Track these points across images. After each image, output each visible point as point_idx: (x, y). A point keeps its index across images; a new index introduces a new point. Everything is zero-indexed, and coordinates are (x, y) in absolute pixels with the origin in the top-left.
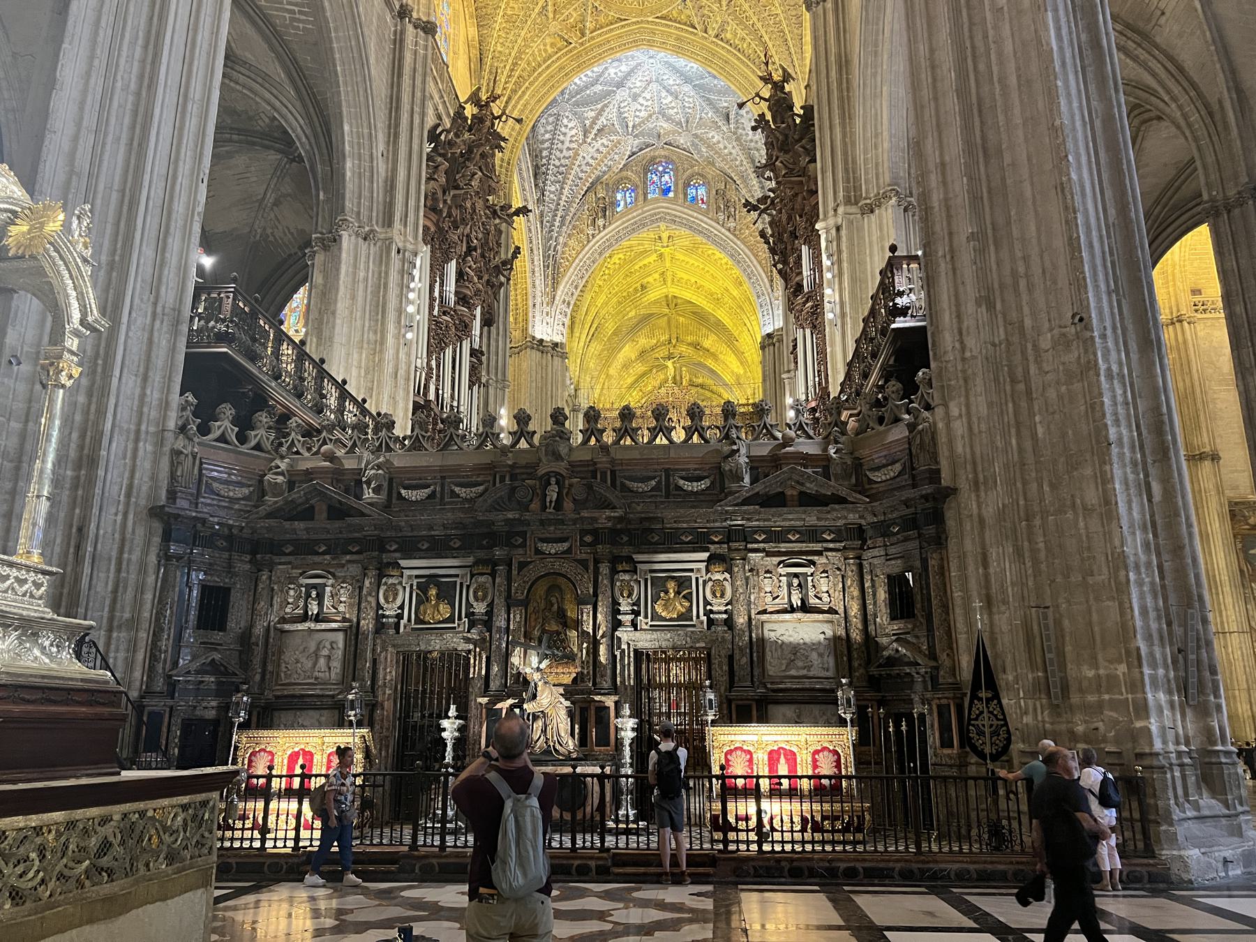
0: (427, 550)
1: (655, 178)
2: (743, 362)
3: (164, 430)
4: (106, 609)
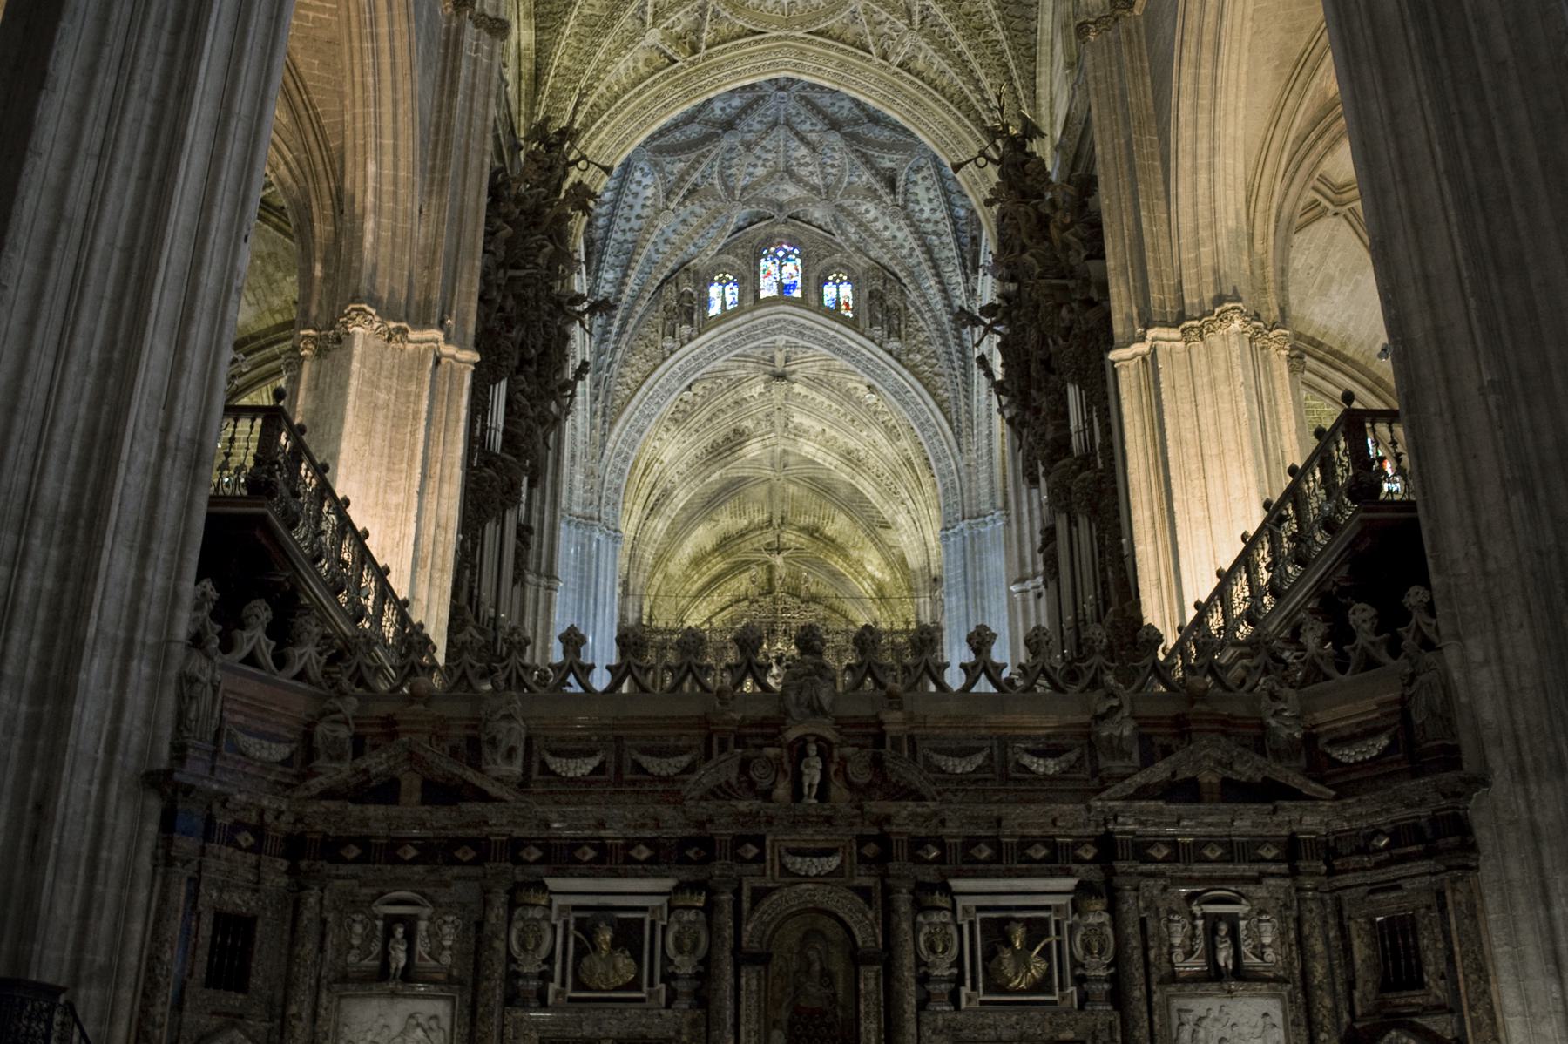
0: (589, 862)
1: (774, 269)
3: (169, 641)
4: (69, 946)
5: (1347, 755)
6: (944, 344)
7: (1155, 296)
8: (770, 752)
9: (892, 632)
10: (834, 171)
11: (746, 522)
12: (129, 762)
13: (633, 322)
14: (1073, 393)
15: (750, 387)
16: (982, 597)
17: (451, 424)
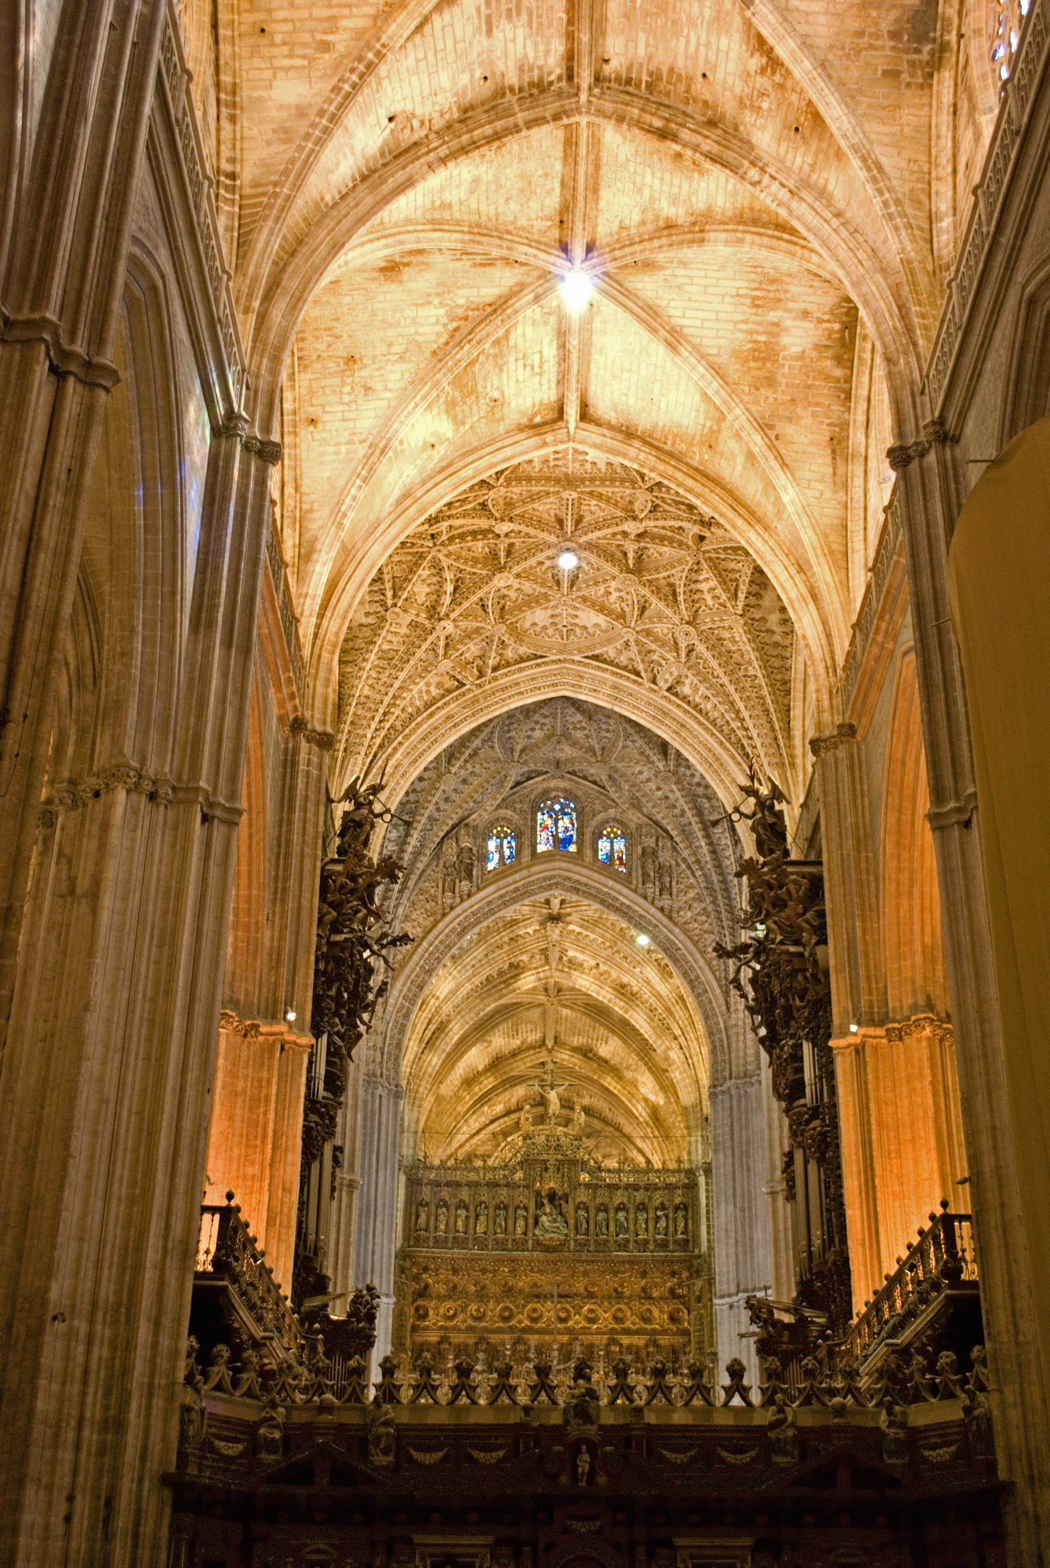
1: (549, 822)
2: (667, 1087)
7: (864, 998)
9: (665, 1170)
10: (609, 735)
11: (518, 1042)
12: (153, 1466)
14: (807, 1050)
15: (526, 927)
16: (748, 1157)
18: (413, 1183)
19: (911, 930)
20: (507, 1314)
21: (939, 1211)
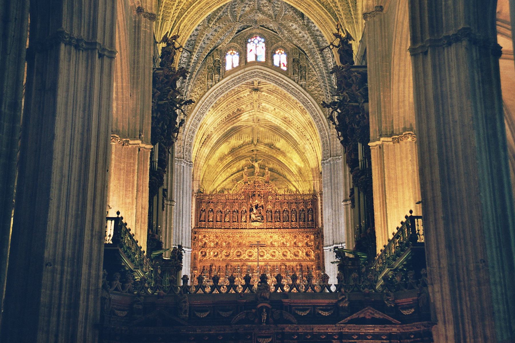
1: (253, 48)
2: (305, 160)
5: (405, 312)
6: (323, 82)
7: (384, 125)
8: (254, 311)
9: (303, 195)
10: (278, 9)
11: (242, 142)
13: (195, 73)
14: (360, 146)
16: (337, 189)
17: (145, 172)
18: (199, 203)
19: (404, 96)
20: (239, 254)
21: (409, 215)
